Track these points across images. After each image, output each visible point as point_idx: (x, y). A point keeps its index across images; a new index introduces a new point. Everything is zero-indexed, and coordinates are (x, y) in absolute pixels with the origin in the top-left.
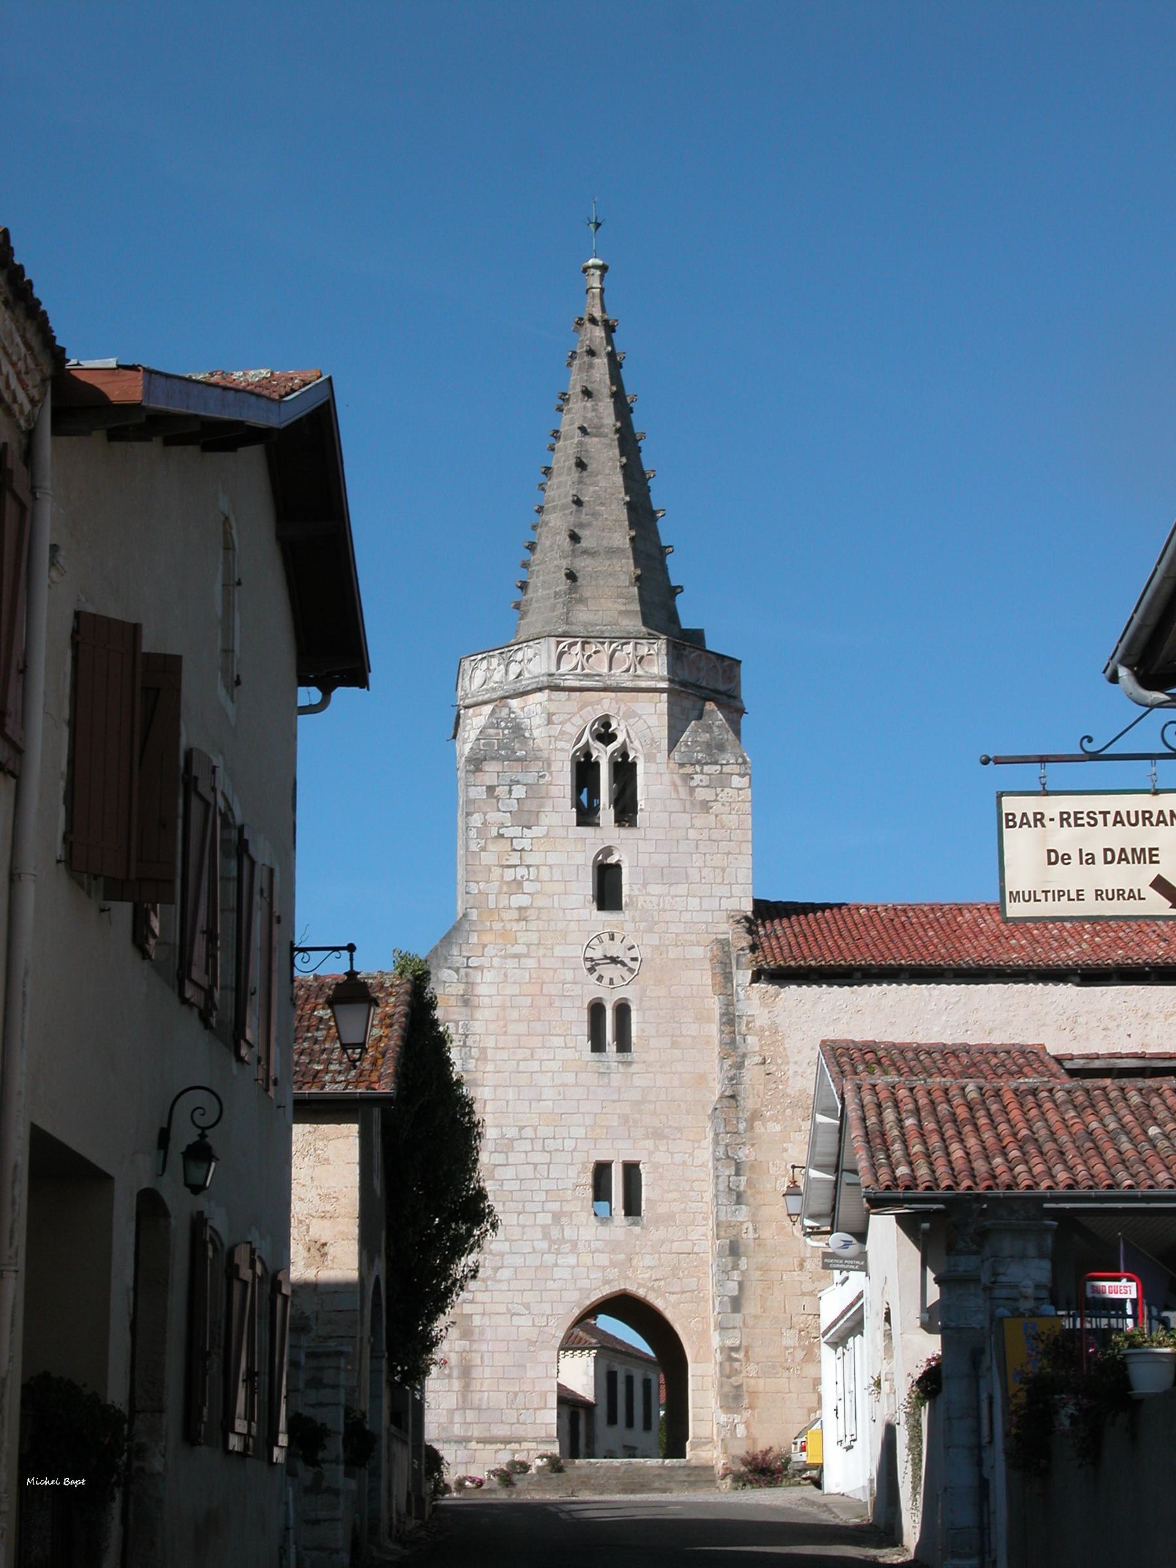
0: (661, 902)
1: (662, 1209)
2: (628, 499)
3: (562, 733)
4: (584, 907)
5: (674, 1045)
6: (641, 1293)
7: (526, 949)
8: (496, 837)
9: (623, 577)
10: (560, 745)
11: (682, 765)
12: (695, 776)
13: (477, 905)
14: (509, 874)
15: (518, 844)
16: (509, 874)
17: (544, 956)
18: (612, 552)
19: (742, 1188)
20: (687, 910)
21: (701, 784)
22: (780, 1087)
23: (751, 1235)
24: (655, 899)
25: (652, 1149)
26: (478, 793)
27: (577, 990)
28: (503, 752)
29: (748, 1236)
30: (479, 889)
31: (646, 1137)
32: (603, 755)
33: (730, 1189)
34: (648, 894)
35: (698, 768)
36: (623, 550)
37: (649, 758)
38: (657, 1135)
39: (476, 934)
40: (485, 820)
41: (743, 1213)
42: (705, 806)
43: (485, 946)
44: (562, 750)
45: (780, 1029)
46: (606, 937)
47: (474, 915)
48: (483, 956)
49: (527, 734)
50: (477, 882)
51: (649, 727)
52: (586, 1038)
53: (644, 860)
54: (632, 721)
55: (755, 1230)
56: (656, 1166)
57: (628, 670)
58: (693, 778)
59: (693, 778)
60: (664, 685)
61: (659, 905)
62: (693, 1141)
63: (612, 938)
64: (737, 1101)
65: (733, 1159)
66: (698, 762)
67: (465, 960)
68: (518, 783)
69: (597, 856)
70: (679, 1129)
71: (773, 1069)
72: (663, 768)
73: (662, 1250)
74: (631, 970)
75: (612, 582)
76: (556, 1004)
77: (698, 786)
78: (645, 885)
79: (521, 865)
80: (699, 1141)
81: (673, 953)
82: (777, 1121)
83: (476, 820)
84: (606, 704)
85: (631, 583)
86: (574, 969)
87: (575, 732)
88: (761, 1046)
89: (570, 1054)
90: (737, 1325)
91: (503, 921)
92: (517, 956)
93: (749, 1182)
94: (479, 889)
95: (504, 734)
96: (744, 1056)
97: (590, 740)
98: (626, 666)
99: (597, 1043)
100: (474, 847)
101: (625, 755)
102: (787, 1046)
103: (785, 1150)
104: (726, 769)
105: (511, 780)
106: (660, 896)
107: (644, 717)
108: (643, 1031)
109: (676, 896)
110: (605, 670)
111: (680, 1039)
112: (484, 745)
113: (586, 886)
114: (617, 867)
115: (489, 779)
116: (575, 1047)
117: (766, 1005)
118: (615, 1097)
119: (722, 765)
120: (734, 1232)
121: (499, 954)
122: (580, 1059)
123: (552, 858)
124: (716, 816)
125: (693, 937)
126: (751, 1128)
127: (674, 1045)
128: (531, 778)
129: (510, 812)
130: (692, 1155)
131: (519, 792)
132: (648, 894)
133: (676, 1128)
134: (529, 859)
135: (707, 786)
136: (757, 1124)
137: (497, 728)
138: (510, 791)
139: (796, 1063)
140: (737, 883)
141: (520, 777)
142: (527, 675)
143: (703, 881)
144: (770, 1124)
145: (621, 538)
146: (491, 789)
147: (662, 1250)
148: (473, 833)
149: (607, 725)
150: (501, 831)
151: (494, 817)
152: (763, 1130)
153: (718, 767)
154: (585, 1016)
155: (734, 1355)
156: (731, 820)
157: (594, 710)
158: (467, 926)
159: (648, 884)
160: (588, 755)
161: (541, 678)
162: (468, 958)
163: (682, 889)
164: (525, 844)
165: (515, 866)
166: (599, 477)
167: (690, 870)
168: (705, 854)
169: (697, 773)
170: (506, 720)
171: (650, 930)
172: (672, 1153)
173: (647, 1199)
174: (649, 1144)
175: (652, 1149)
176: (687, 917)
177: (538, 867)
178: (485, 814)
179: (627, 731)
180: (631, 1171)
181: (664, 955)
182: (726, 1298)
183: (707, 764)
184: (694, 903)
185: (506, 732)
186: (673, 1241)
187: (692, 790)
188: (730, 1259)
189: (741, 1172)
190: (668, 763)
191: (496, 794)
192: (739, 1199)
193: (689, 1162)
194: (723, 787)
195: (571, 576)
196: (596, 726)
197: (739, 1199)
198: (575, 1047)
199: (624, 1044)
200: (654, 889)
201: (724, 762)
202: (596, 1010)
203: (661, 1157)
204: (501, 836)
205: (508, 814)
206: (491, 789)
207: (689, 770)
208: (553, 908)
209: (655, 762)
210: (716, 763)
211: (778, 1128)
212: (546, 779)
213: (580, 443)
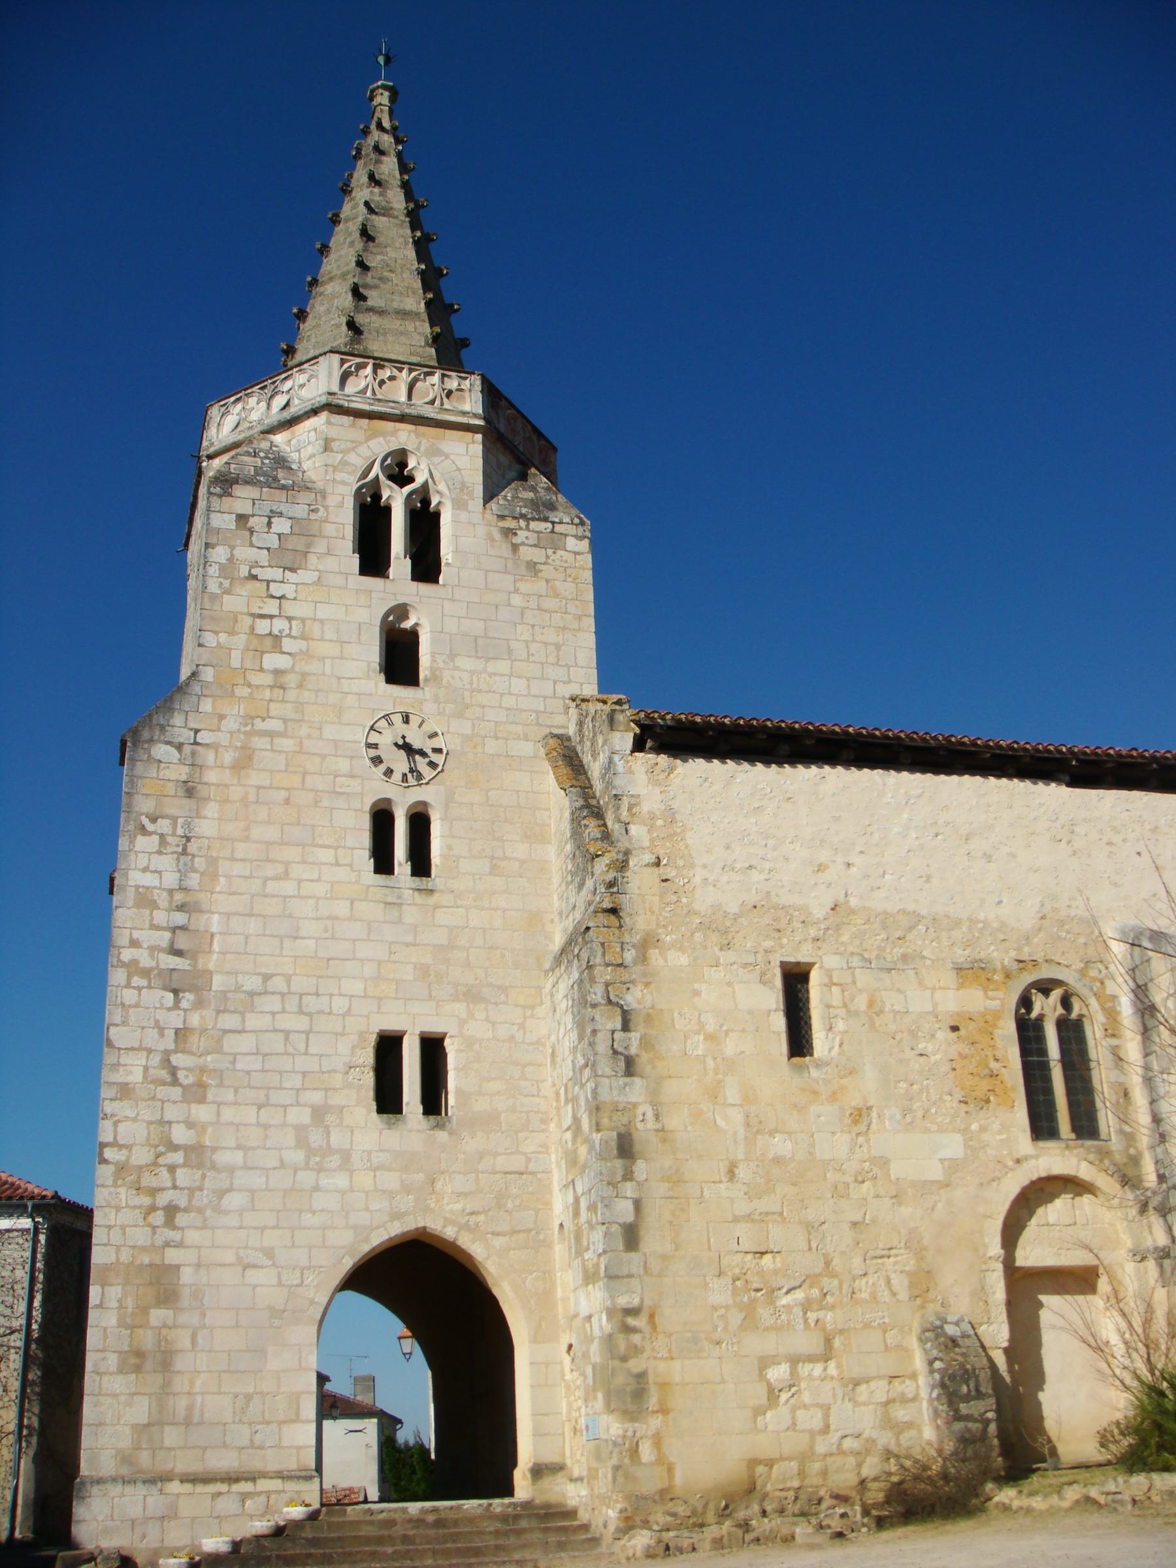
0: (475, 680)
1: (481, 1105)
2: (423, 267)
3: (344, 463)
4: (368, 677)
5: (494, 870)
6: (449, 1233)
7: (283, 726)
8: (246, 578)
9: (417, 337)
10: (339, 476)
11: (502, 517)
12: (518, 532)
13: (214, 662)
14: (263, 627)
15: (275, 589)
16: (263, 627)
17: (309, 737)
18: (404, 314)
19: (633, 1051)
20: (510, 694)
21: (526, 542)
22: (684, 900)
23: (651, 1124)
24: (465, 676)
25: (464, 1015)
26: (227, 522)
27: (355, 786)
28: (262, 479)
29: (645, 1128)
30: (218, 642)
31: (455, 998)
32: (397, 500)
33: (615, 1052)
34: (457, 668)
35: (522, 523)
36: (417, 314)
37: (459, 505)
38: (472, 996)
39: (210, 700)
40: (232, 555)
41: (637, 1091)
42: (533, 567)
43: (222, 717)
44: (343, 483)
45: (678, 817)
46: (397, 719)
47: (208, 674)
48: (219, 729)
49: (294, 467)
50: (216, 633)
51: (459, 469)
52: (366, 854)
53: (451, 626)
54: (436, 460)
55: (657, 1117)
56: (469, 1043)
57: (432, 402)
58: (515, 534)
59: (515, 534)
60: (481, 423)
61: (471, 683)
62: (524, 1007)
63: (406, 720)
64: (619, 918)
65: (618, 1005)
66: (523, 516)
67: (192, 734)
68: (281, 515)
69: (387, 615)
70: (503, 989)
71: (671, 873)
72: (477, 517)
73: (481, 1167)
74: (432, 765)
75: (403, 339)
76: (326, 803)
77: (523, 544)
78: (452, 656)
79: (280, 616)
80: (533, 1007)
81: (492, 746)
82: (681, 949)
83: (220, 554)
84: (404, 436)
85: (427, 344)
86: (352, 758)
87: (362, 464)
88: (652, 840)
89: (342, 874)
90: (634, 1271)
91: (250, 686)
92: (271, 734)
93: (645, 1043)
94: (218, 642)
95: (262, 463)
96: (627, 853)
97: (382, 478)
98: (431, 397)
99: (383, 863)
100: (213, 587)
101: (426, 502)
102: (689, 841)
103: (697, 993)
104: (558, 528)
105: (271, 511)
106: (472, 672)
107: (452, 457)
108: (450, 848)
109: (495, 674)
110: (403, 398)
111: (503, 864)
112: (235, 469)
113: (372, 652)
114: (412, 637)
115: (244, 507)
116: (351, 865)
117: (657, 783)
118: (409, 938)
119: (553, 523)
120: (625, 1120)
121: (243, 729)
122: (357, 882)
123: (323, 612)
124: (547, 581)
125: (519, 729)
126: (643, 958)
127: (494, 870)
128: (300, 511)
129: (268, 549)
130: (522, 1026)
131: (281, 526)
132: (457, 668)
133: (499, 987)
134: (290, 609)
135: (535, 546)
136: (653, 953)
137: (255, 456)
138: (269, 524)
139: (705, 866)
140: (577, 665)
141: (283, 508)
142: (296, 401)
143: (531, 659)
144: (672, 955)
145: (416, 302)
146: (242, 518)
147: (481, 1167)
148: (213, 570)
149: (403, 465)
150: (254, 572)
151: (245, 553)
152: (661, 962)
153: (549, 525)
154: (366, 823)
155: (631, 1321)
156: (566, 588)
157: (387, 442)
158: (196, 688)
159: (456, 655)
160: (377, 496)
161: (318, 399)
162: (197, 731)
163: (503, 666)
164: (287, 590)
165: (271, 617)
166: (388, 249)
167: (514, 645)
168: (533, 626)
169: (521, 529)
170: (267, 452)
171: (460, 715)
172: (493, 1024)
173: (459, 1091)
174: (460, 1008)
175: (464, 1015)
176: (509, 702)
177: (303, 620)
178: (232, 548)
179: (430, 470)
180: (433, 1049)
181: (480, 750)
182: (615, 1227)
183: (533, 519)
184: (519, 685)
185: (267, 461)
186: (496, 1154)
187: (515, 548)
188: (619, 1163)
189: (632, 1025)
190: (483, 513)
191: (250, 524)
192: (630, 1067)
193: (519, 1036)
194: (556, 549)
195: (352, 325)
196: (389, 461)
197: (630, 1067)
198: (351, 865)
199: (421, 864)
200: (466, 663)
201: (557, 520)
202: (382, 819)
203: (477, 1029)
204: (255, 577)
205: (265, 552)
206: (242, 518)
207: (510, 523)
208: (324, 674)
209: (467, 510)
210: (546, 520)
211: (684, 960)
212: (320, 514)
213: (366, 219)
